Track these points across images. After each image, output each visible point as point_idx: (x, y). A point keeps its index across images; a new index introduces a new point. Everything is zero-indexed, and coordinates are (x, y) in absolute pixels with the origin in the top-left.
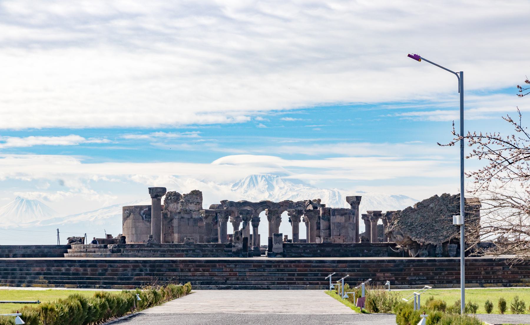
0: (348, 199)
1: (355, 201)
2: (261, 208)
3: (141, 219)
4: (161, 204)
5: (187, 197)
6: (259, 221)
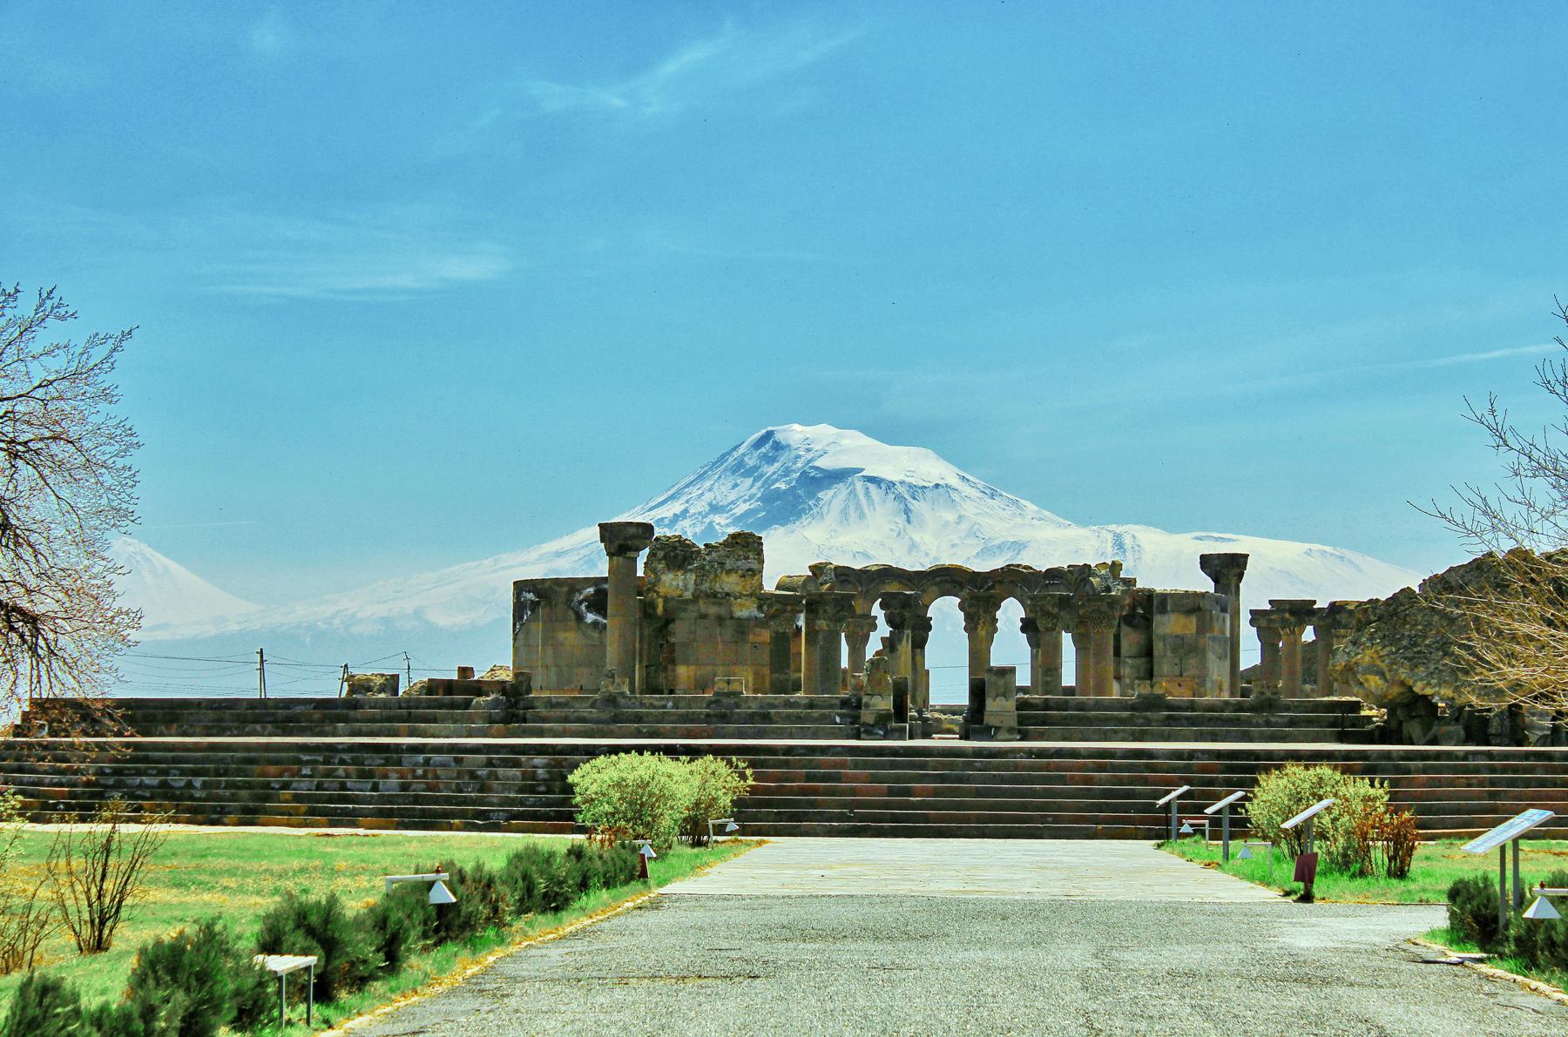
0: (1206, 562)
1: (1226, 569)
2: (934, 588)
3: (571, 620)
4: (638, 575)
5: (715, 552)
6: (930, 628)
